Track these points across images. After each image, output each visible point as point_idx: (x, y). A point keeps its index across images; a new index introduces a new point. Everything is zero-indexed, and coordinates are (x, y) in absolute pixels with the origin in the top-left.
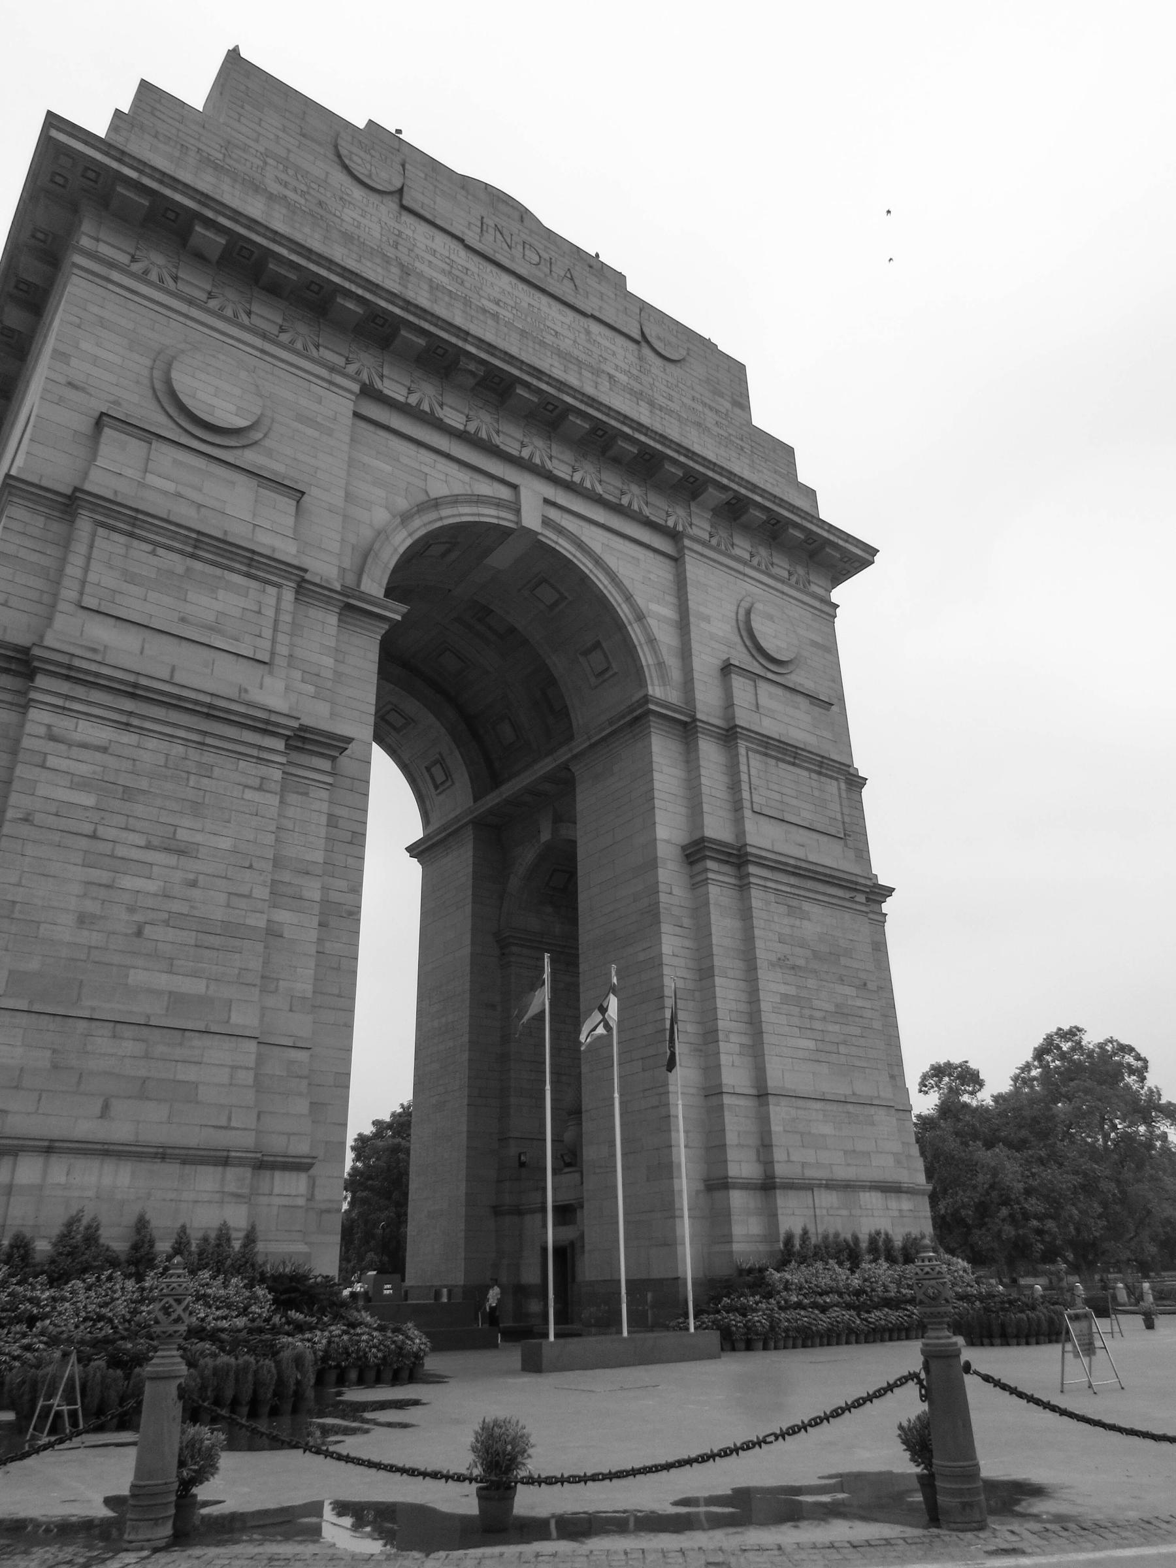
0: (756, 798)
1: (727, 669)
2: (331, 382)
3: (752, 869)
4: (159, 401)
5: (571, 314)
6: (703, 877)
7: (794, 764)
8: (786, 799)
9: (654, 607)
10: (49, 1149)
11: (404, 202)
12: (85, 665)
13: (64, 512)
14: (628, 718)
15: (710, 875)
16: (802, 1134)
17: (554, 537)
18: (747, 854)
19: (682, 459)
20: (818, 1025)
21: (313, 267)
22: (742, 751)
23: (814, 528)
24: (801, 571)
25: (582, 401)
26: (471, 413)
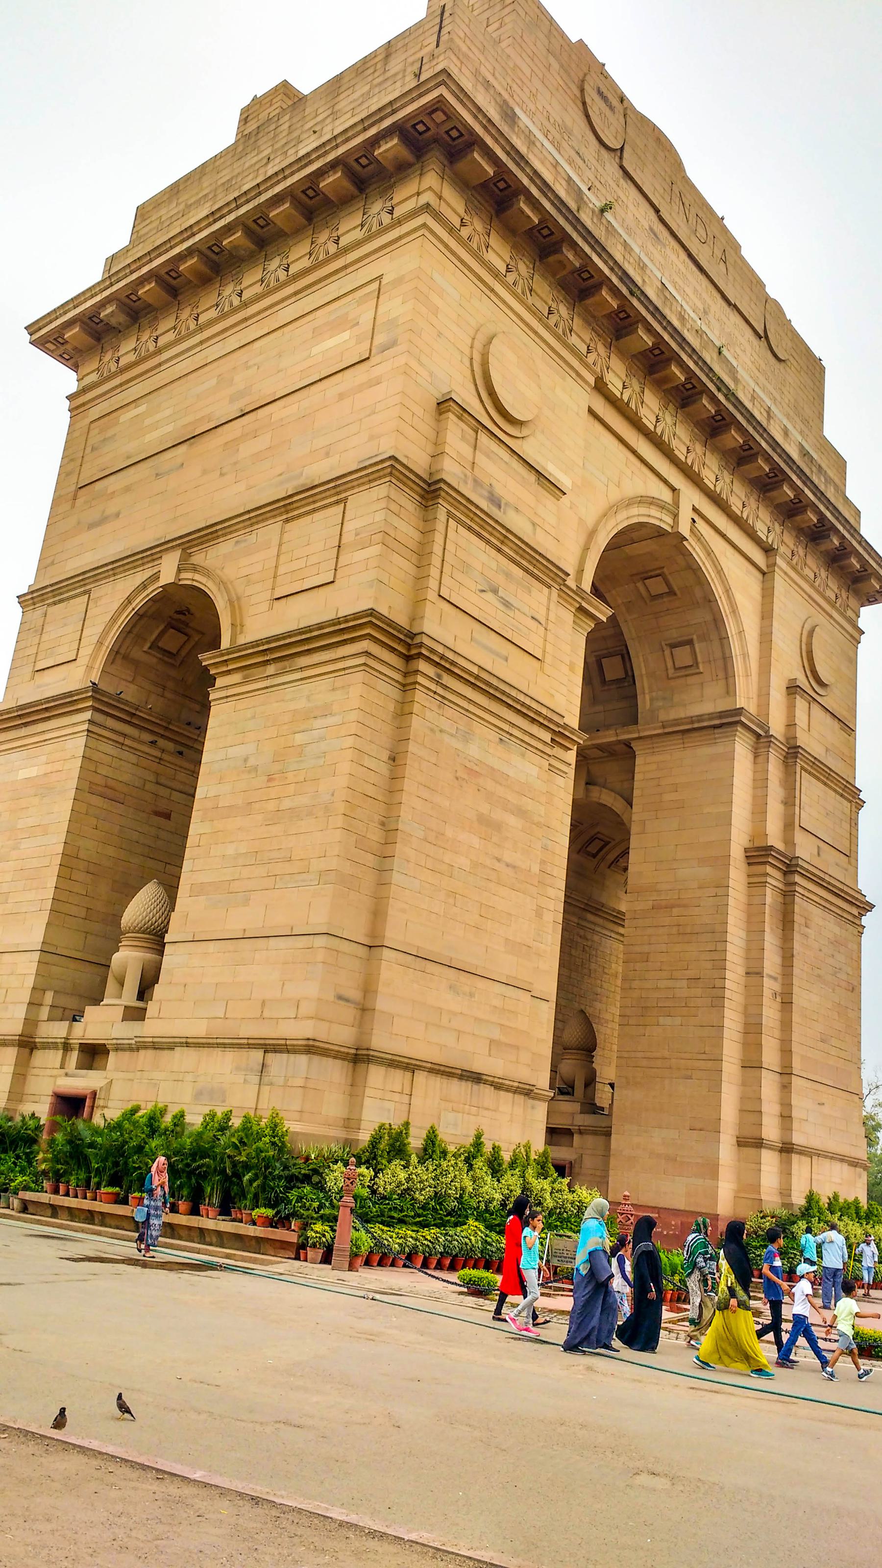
1: (793, 689)
2: (578, 374)
3: (797, 879)
4: (476, 385)
6: (763, 879)
11: (625, 164)
12: (450, 655)
13: (422, 497)
14: (717, 722)
15: (769, 880)
17: (693, 543)
18: (797, 865)
22: (798, 769)
24: (844, 594)
26: (661, 414)
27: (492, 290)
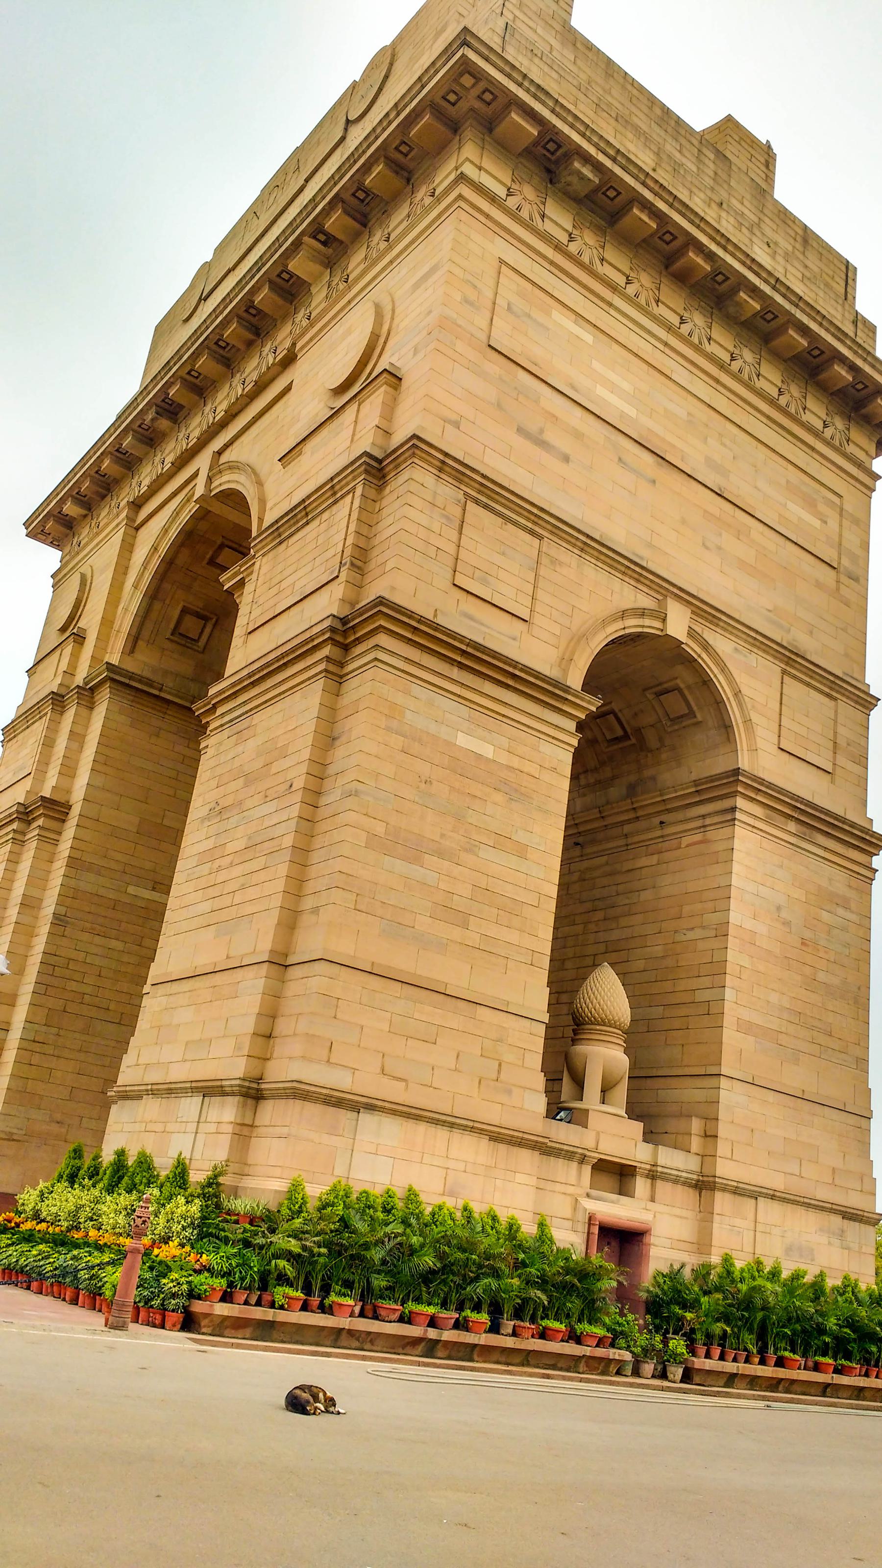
0: (253, 617)
7: (307, 523)
24: (422, 193)
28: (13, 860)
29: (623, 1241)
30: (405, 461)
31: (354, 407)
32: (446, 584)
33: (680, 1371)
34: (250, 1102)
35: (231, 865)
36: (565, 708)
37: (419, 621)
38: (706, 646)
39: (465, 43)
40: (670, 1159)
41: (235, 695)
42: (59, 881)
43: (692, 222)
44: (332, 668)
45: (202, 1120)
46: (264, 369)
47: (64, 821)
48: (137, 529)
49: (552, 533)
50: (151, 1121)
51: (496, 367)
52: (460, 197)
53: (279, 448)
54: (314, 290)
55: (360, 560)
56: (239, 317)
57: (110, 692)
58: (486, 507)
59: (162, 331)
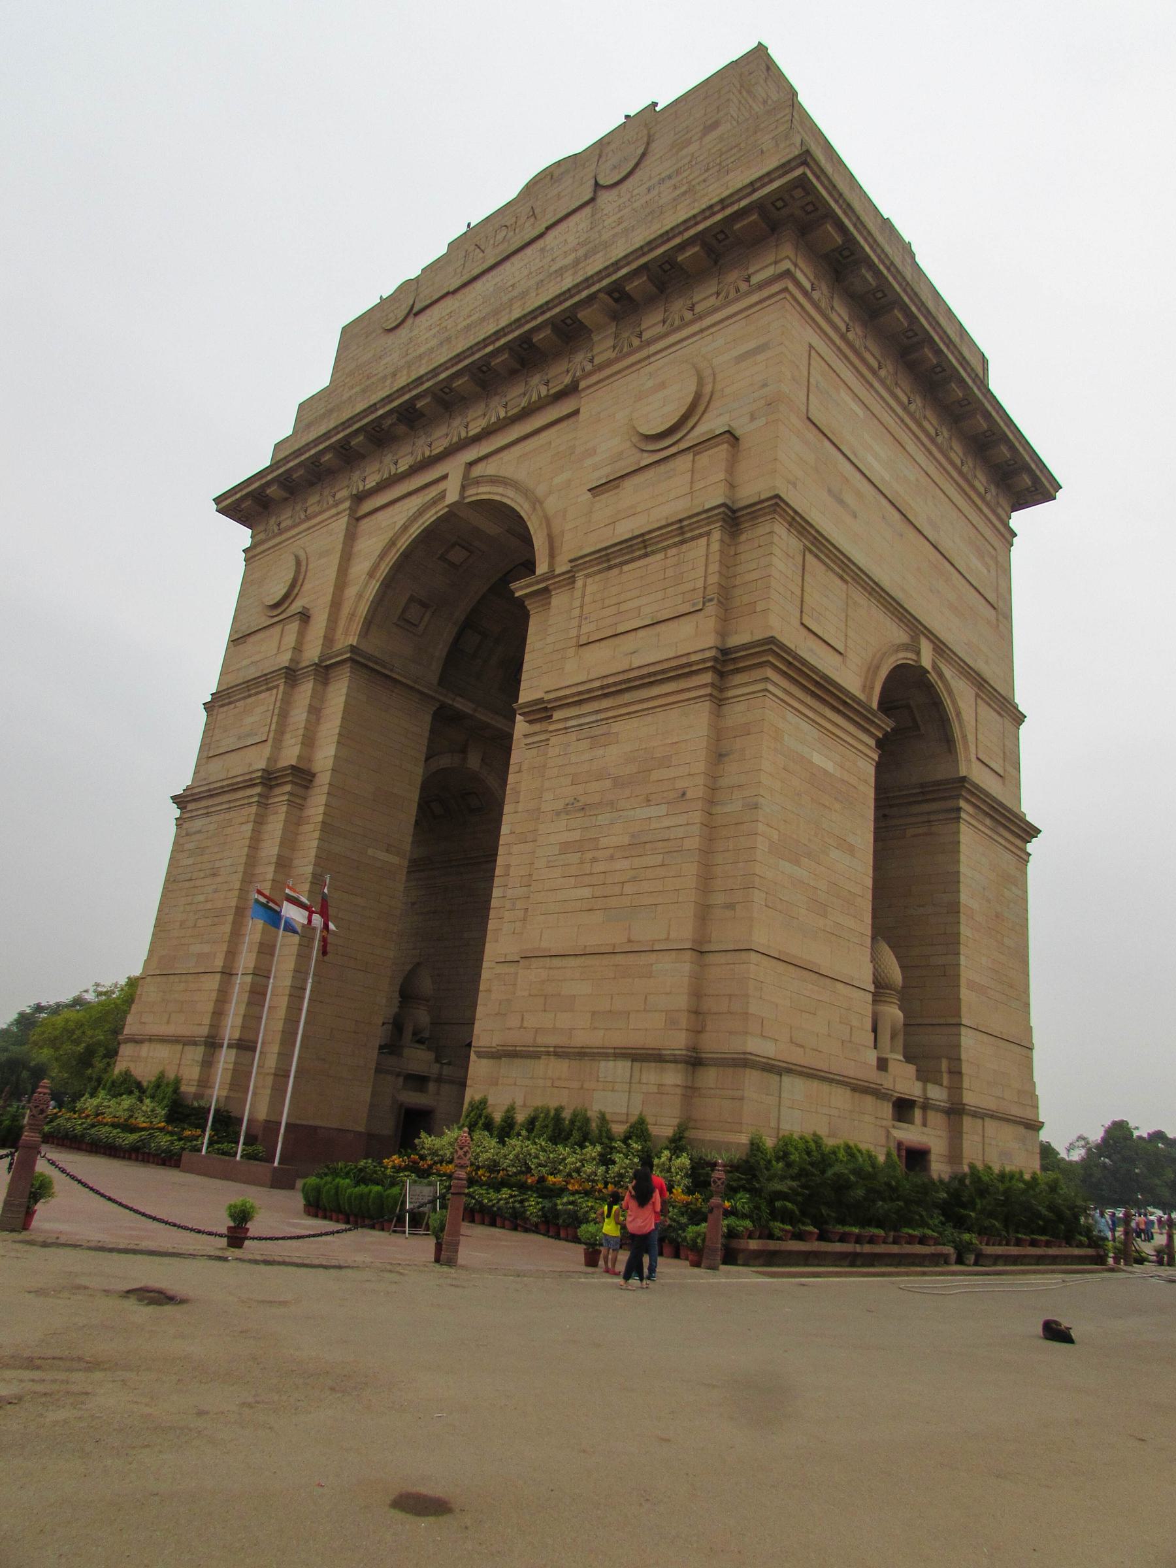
0: (584, 630)
5: (529, 251)
7: (646, 555)
8: (623, 607)
9: (557, 480)
10: (150, 1040)
16: (546, 996)
19: (540, 320)
20: (600, 867)
21: (303, 458)
22: (579, 584)
23: (701, 227)
24: (733, 276)
25: (453, 366)
27: (280, 543)
28: (260, 821)
29: (916, 1157)
30: (765, 514)
31: (690, 456)
32: (797, 623)
33: (972, 1258)
34: (690, 1068)
35: (612, 858)
36: (872, 729)
37: (794, 658)
38: (941, 675)
39: (804, 163)
40: (937, 1094)
41: (579, 703)
42: (315, 843)
43: (930, 324)
44: (715, 693)
45: (636, 1079)
46: (534, 397)
47: (307, 788)
48: (358, 519)
49: (853, 579)
50: (559, 1079)
51: (811, 435)
52: (786, 290)
53: (562, 472)
54: (596, 338)
55: (725, 599)
56: (511, 349)
57: (351, 672)
58: (816, 556)
59: (353, 335)
